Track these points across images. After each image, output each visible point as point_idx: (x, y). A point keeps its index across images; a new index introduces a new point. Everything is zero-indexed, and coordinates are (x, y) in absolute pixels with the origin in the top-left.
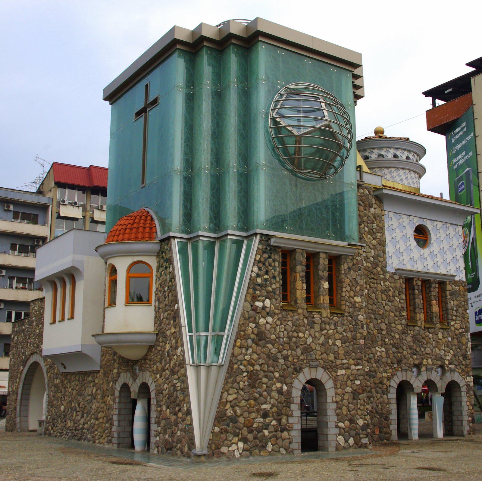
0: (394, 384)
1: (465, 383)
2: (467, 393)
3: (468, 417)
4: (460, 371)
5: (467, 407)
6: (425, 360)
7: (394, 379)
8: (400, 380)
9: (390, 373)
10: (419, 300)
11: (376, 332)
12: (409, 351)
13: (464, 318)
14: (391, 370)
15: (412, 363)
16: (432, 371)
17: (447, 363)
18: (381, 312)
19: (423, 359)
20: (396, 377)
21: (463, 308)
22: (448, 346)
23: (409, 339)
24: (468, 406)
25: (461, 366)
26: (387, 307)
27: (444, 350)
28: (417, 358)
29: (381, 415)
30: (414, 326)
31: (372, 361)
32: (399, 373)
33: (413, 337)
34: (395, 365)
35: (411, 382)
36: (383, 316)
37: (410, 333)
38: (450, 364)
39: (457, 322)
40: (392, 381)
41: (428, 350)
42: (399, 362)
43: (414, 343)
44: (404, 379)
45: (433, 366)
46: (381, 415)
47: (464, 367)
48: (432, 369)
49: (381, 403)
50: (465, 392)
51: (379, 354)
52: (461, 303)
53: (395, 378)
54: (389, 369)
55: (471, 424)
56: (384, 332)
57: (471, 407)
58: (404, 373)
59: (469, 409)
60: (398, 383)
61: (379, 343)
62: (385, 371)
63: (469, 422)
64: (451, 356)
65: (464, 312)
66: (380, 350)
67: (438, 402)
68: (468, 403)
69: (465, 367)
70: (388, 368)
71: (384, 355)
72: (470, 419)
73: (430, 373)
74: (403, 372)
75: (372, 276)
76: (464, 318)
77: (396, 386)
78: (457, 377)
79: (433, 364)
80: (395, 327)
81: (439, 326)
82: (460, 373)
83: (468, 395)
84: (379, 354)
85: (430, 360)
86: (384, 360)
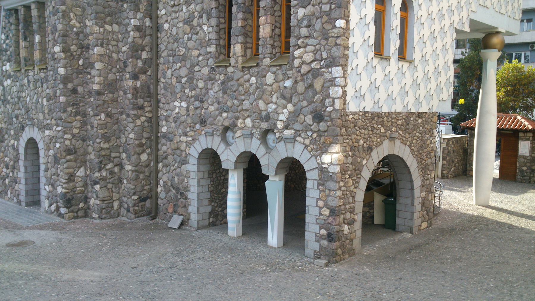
0: (195, 152)
1: (317, 166)
2: (319, 185)
3: (318, 227)
4: (307, 142)
5: (317, 209)
6: (240, 121)
7: (195, 145)
8: (204, 148)
9: (191, 136)
10: (237, 23)
11: (174, 80)
12: (216, 105)
13: (327, 39)
14: (192, 133)
15: (220, 124)
16: (252, 138)
17: (280, 125)
18: (183, 51)
19: (237, 118)
20: (197, 142)
21: (325, 18)
22: (283, 97)
23: (216, 88)
24: (321, 208)
25: (310, 133)
26: (191, 44)
27: (276, 103)
28: (227, 118)
29: (177, 189)
30: (226, 67)
31: (171, 119)
32: (202, 138)
33: (223, 83)
34: (198, 126)
35: (219, 152)
36: (184, 58)
37: (219, 79)
38: (286, 127)
39: (309, 48)
40: (192, 148)
41: (246, 104)
42: (203, 122)
43: (225, 92)
44: (209, 147)
45: (254, 131)
46: (177, 189)
47: (315, 135)
48: (252, 134)
49: (177, 175)
50: (316, 182)
51: (177, 110)
52: (321, 8)
53: (197, 144)
54: (191, 130)
55: (325, 243)
56: (184, 80)
57: (326, 212)
58: (209, 138)
59: (321, 214)
60: (200, 151)
61: (178, 96)
62: (185, 134)
63: (319, 238)
64: (287, 115)
65: (328, 27)
66: (178, 105)
67: (275, 189)
68: (321, 203)
69: (320, 136)
70: (188, 129)
71: (183, 112)
72: (324, 232)
73: (249, 141)
74: (208, 137)
75: (172, 3)
76: (327, 39)
77: (197, 156)
78: (298, 152)
79: (253, 127)
80: (200, 71)
81: (267, 61)
82: (306, 146)
83: (321, 187)
84: (177, 110)
85: (248, 122)
86: (183, 119)
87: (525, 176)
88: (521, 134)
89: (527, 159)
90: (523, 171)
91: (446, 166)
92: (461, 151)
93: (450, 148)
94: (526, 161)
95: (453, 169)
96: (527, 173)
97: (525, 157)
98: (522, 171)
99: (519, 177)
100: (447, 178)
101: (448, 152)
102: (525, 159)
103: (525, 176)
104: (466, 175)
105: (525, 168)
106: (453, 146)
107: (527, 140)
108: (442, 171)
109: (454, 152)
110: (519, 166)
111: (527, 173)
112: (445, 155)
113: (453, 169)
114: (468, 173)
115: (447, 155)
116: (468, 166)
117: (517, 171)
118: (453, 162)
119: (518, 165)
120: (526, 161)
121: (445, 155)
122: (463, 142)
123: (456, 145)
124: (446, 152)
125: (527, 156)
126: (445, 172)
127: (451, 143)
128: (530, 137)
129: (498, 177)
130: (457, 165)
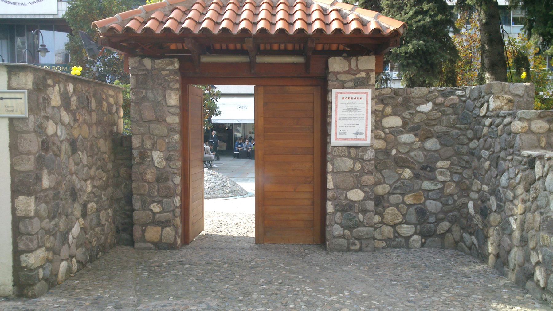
87: (360, 224)
88: (336, 64)
89: (362, 160)
90: (351, 204)
91: (36, 226)
92: (104, 146)
93: (51, 128)
94: (358, 166)
95: (76, 230)
96: (364, 211)
97: (354, 152)
98: (347, 207)
99: (337, 230)
100: (52, 283)
101: (46, 145)
102: (356, 159)
103: (360, 224)
104: (131, 243)
105: (356, 195)
106: (66, 118)
107: (360, 84)
108: (17, 253)
109: (73, 143)
110: (337, 187)
111: (364, 211)
112: (28, 165)
113: (76, 230)
114: (137, 233)
115: (41, 162)
116: (137, 204)
117: (330, 208)
118: (74, 194)
119: (330, 185)
120: (358, 166)
121: (28, 165)
122: (110, 112)
123: (82, 116)
124: (31, 143)
125: (364, 149)
126: (31, 260)
127: (55, 97)
128: (368, 72)
129: (252, 234)
130: (92, 206)
